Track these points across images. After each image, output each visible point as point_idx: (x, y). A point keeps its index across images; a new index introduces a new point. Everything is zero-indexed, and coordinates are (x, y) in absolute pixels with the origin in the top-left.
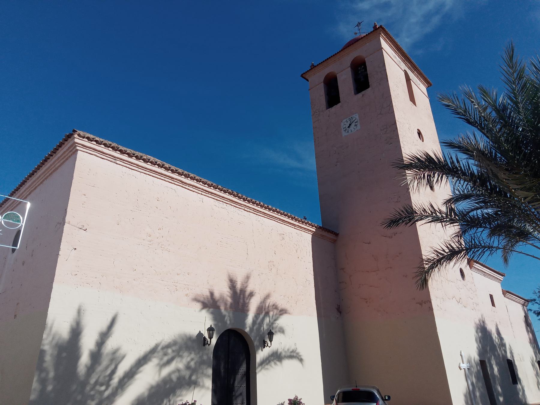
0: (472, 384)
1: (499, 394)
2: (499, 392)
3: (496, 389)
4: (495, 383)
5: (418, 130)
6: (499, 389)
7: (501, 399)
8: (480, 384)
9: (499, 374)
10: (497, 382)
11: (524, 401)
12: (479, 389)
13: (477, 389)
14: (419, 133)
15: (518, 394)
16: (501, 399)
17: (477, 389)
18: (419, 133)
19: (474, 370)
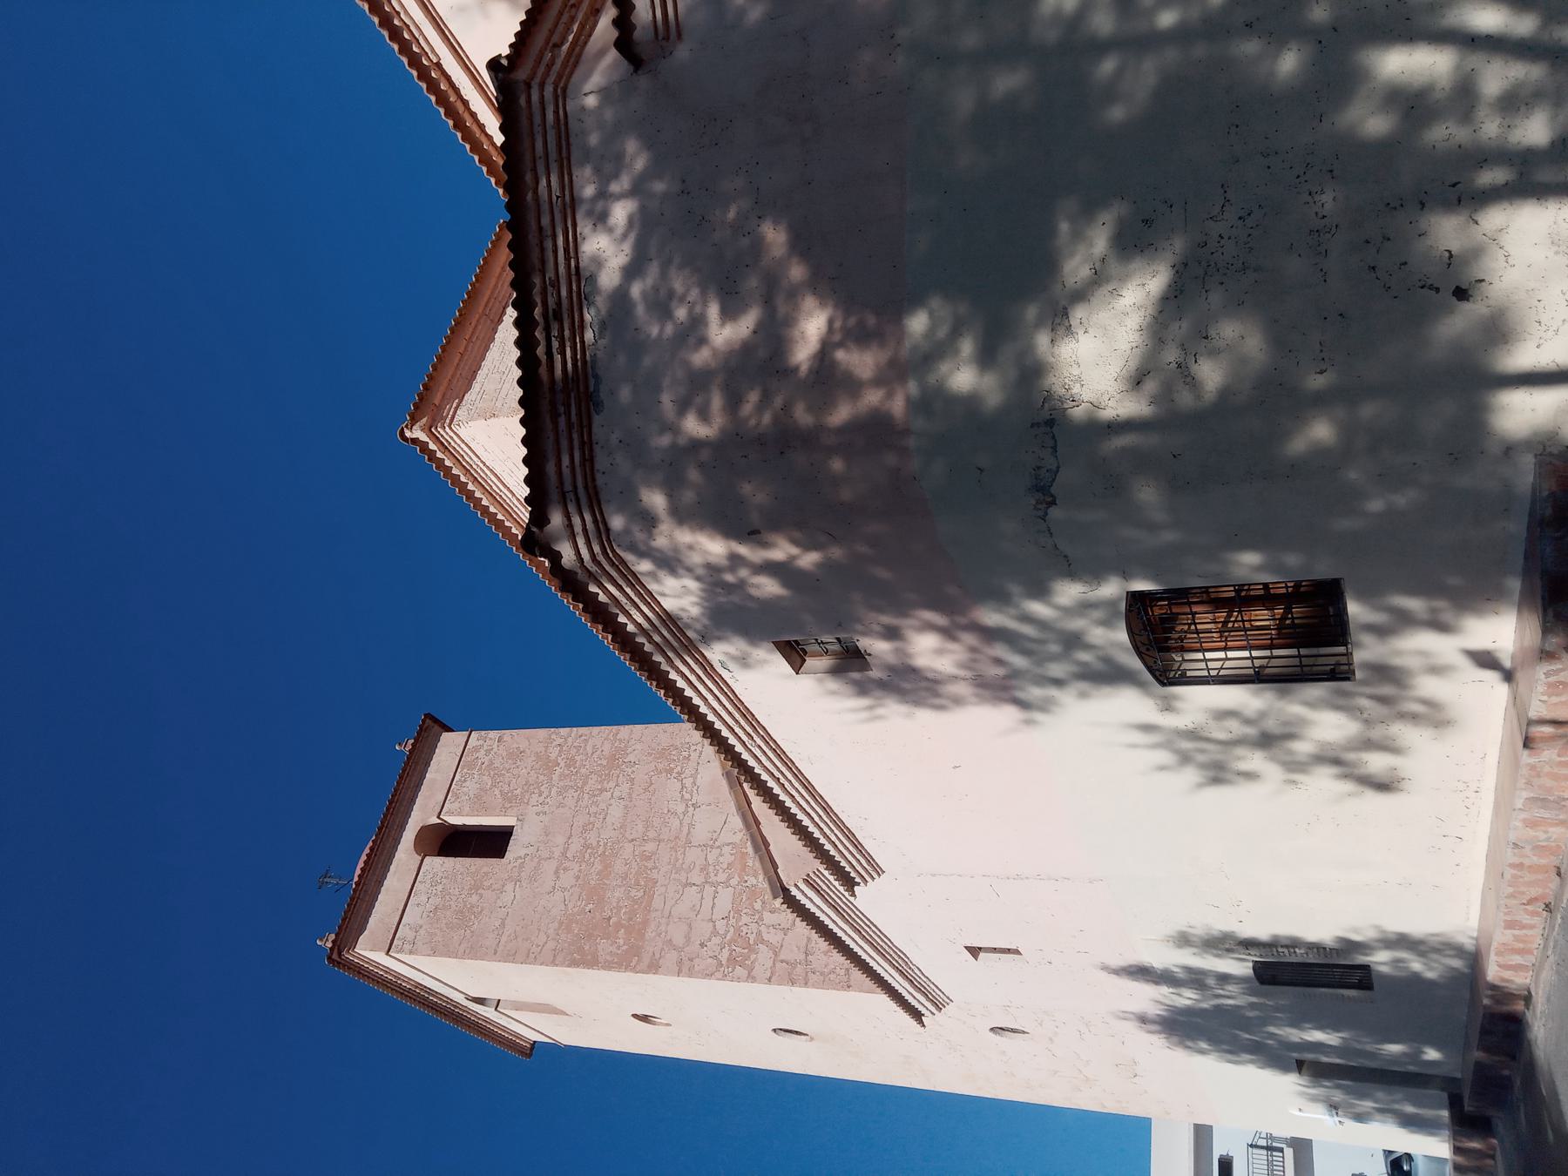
0: (1381, 1111)
1: (1415, 1057)
2: (1404, 1054)
3: (1395, 1059)
4: (1373, 1055)
5: (633, 1015)
6: (1395, 1048)
7: (1432, 1054)
8: (1380, 1095)
9: (1338, 1031)
10: (1369, 1048)
11: (1457, 963)
12: (1394, 1101)
13: (1397, 1106)
14: (644, 1018)
15: (1416, 979)
16: (1432, 1054)
17: (1397, 1106)
18: (644, 1018)
19: (1338, 1096)
